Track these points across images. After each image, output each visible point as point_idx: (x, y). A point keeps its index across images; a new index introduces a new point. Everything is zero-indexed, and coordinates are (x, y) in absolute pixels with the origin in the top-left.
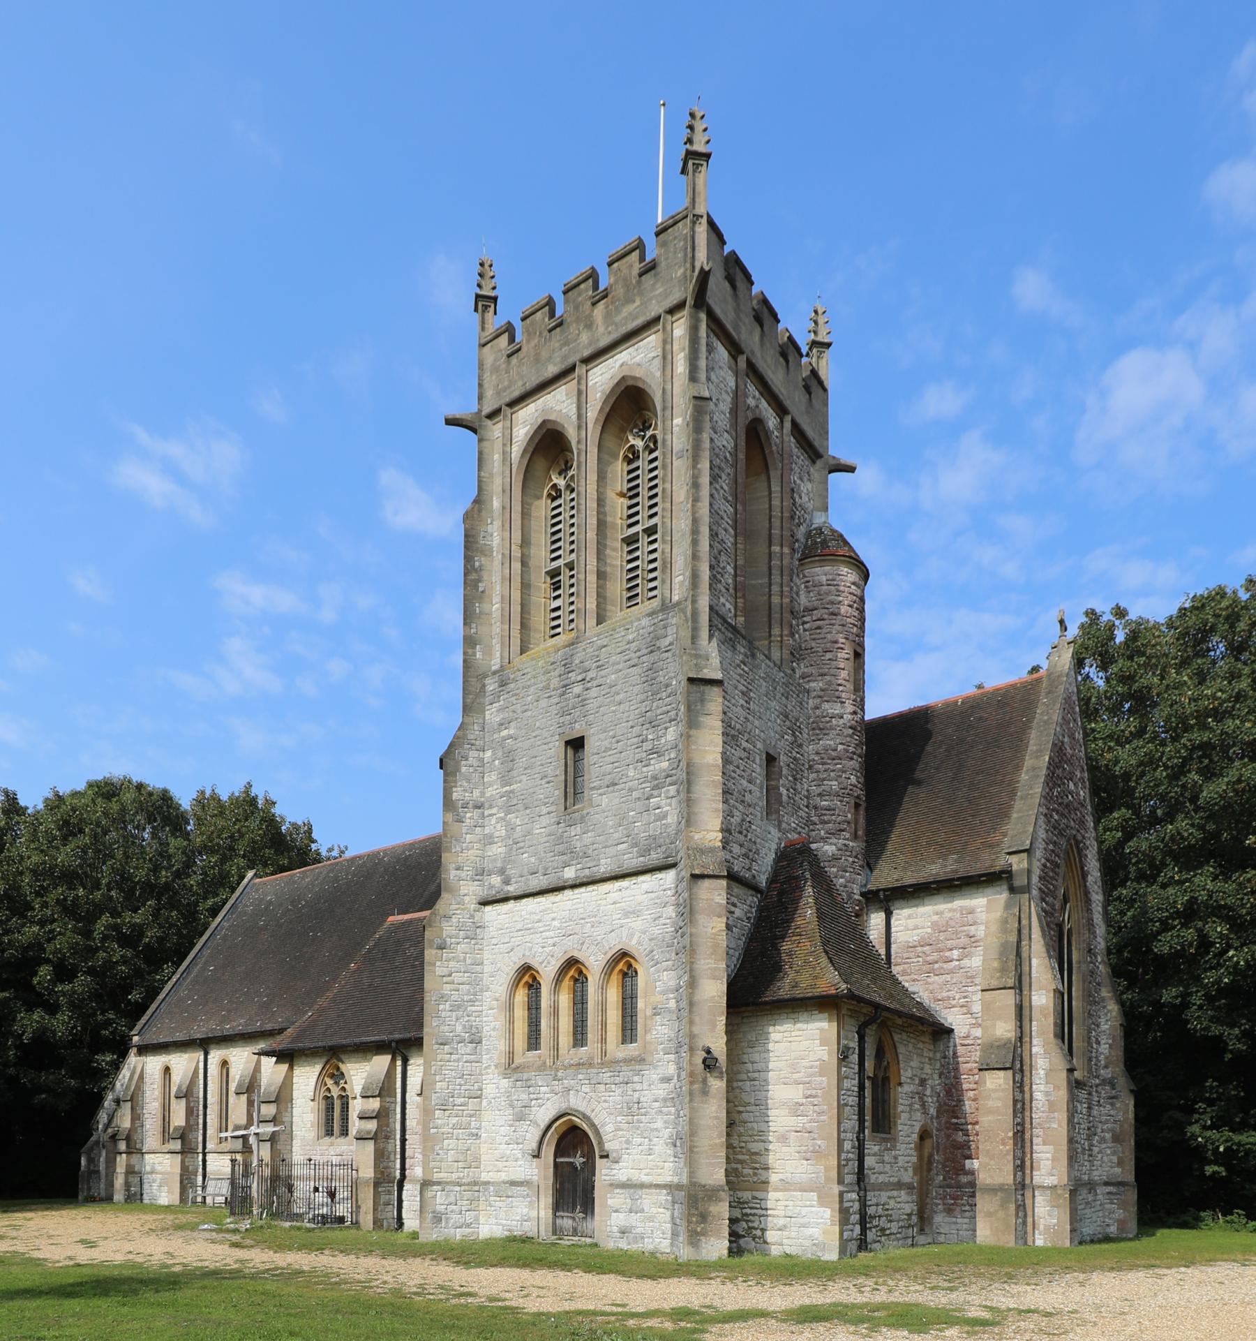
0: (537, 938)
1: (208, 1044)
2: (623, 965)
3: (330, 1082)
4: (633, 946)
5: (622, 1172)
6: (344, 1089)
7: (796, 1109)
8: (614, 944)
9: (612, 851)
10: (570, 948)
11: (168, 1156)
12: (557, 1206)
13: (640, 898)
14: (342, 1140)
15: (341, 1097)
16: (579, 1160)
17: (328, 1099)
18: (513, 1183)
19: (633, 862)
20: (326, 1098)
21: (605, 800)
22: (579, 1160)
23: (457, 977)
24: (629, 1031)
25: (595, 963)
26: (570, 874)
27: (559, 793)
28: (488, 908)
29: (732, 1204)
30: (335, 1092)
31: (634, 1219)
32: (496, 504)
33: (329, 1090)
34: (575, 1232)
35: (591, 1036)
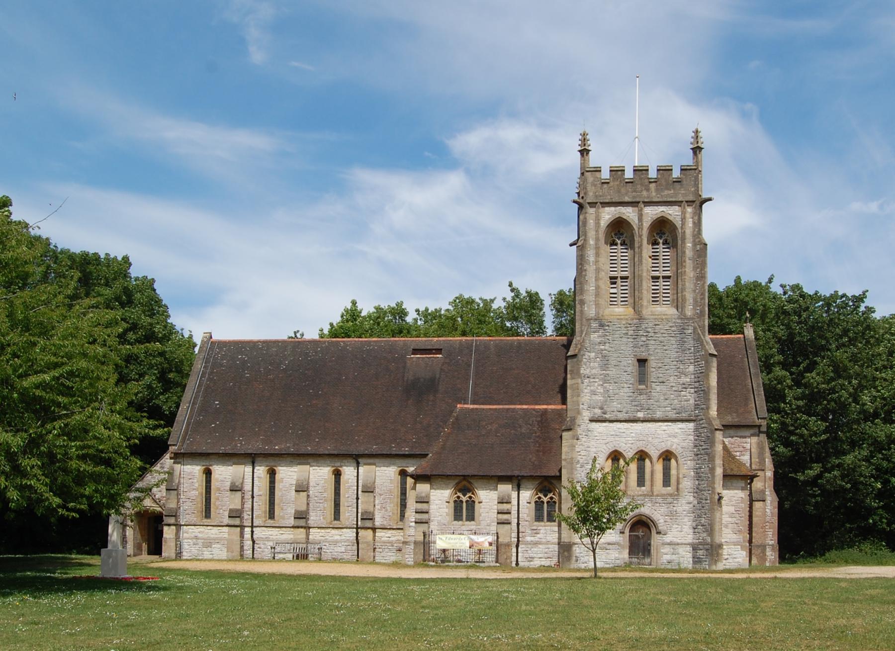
0: (623, 440)
1: (258, 460)
2: (667, 456)
3: (459, 494)
4: (673, 449)
5: (668, 538)
6: (470, 497)
7: (731, 515)
8: (664, 447)
9: (663, 409)
10: (641, 446)
11: (226, 529)
12: (631, 553)
13: (677, 431)
14: (468, 523)
15: (467, 501)
16: (641, 533)
17: (458, 504)
18: (609, 544)
19: (672, 415)
20: (455, 502)
21: (658, 389)
22: (641, 533)
23: (583, 453)
24: (666, 482)
25: (654, 454)
26: (640, 415)
27: (632, 380)
28: (594, 423)
29: (708, 550)
30: (464, 499)
31: (674, 557)
32: (592, 242)
33: (458, 497)
34: (639, 563)
35: (648, 482)
